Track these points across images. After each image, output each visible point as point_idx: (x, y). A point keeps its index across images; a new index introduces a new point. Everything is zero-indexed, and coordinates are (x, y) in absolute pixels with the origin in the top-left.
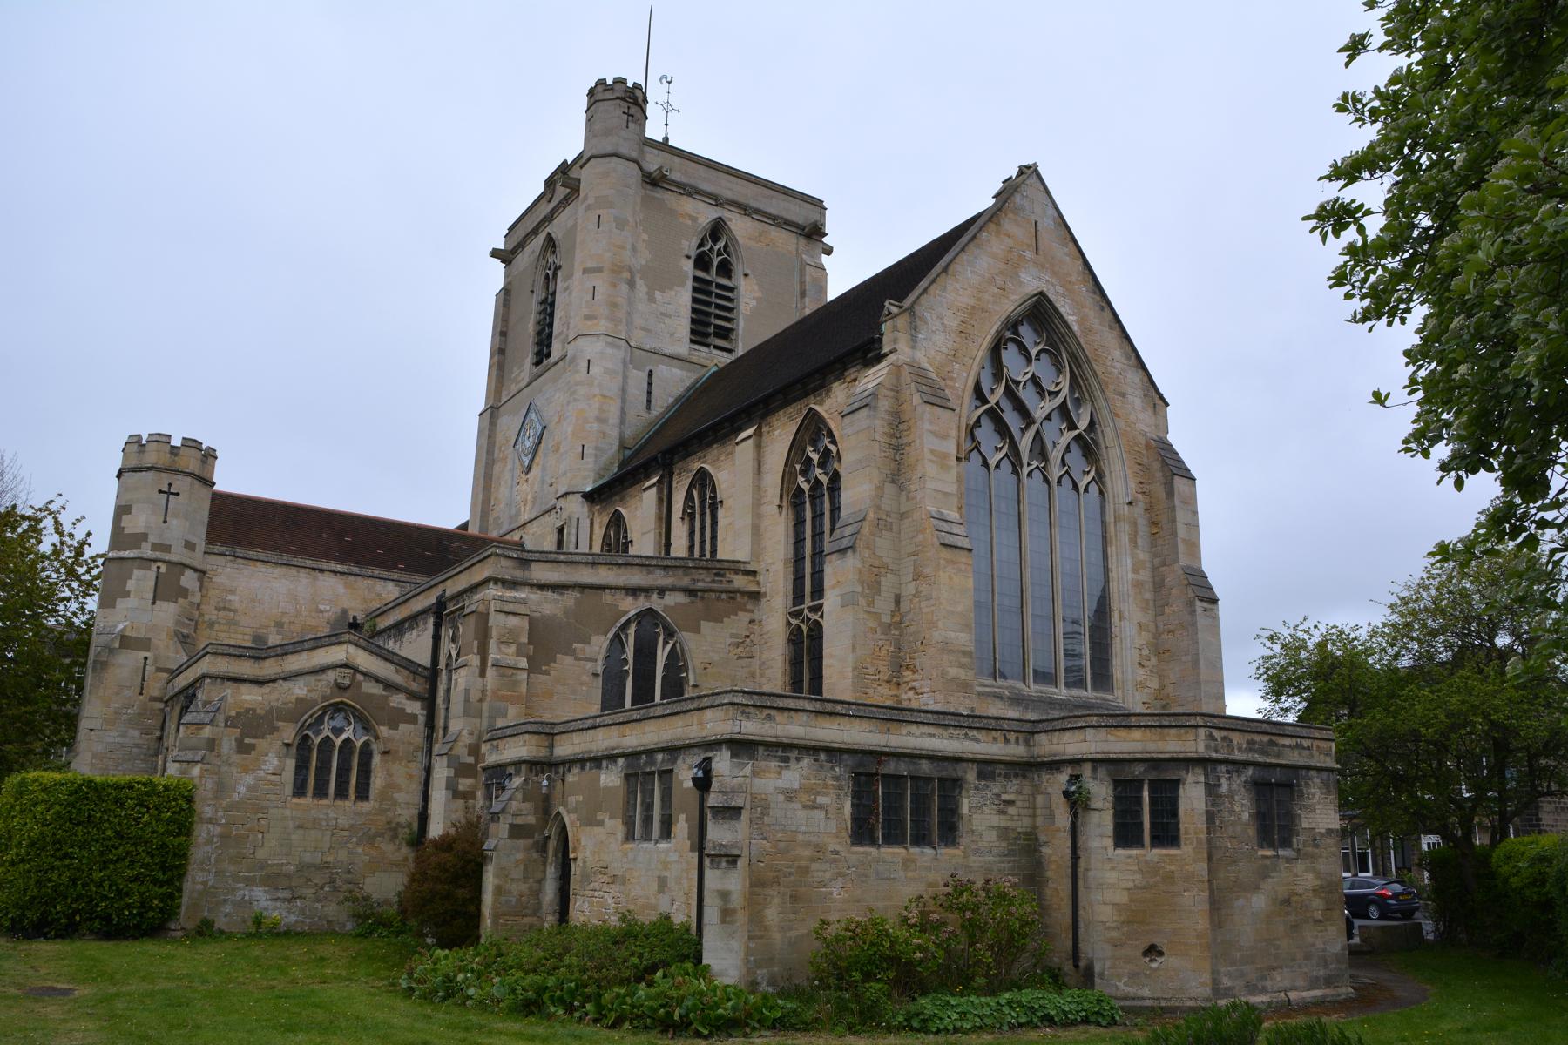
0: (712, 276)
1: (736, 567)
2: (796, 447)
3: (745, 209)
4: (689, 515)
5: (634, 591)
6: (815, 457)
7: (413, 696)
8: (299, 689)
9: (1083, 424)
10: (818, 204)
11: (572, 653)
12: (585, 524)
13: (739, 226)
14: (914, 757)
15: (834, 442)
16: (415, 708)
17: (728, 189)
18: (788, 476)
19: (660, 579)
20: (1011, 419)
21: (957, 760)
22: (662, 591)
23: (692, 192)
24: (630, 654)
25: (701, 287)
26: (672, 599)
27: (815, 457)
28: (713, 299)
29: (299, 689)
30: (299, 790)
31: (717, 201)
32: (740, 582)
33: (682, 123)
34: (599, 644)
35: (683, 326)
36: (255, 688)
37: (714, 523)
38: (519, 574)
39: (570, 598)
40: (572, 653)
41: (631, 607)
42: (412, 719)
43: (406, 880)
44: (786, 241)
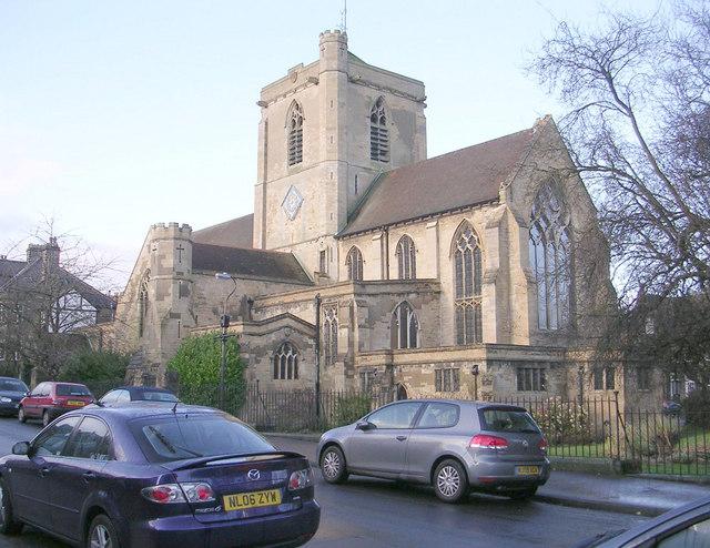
0: (378, 125)
1: (427, 282)
2: (458, 234)
3: (391, 91)
4: (399, 254)
5: (399, 295)
6: (467, 240)
7: (311, 337)
8: (273, 337)
9: (567, 223)
10: (421, 84)
11: (380, 320)
12: (334, 250)
13: (389, 98)
14: (532, 362)
15: (475, 233)
16: (311, 342)
17: (382, 81)
18: (454, 245)
19: (408, 288)
20: (543, 225)
21: (545, 362)
22: (409, 293)
23: (366, 84)
24: (399, 319)
25: (374, 131)
26: (412, 296)
27: (467, 240)
28: (379, 137)
29: (273, 337)
30: (276, 377)
31: (379, 88)
32: (434, 287)
33: (353, 47)
34: (390, 315)
35: (369, 156)
36: (259, 338)
37: (414, 263)
38: (362, 291)
39: (379, 299)
40: (380, 320)
41: (399, 300)
42: (311, 346)
43: (102, 435)
44: (408, 105)
